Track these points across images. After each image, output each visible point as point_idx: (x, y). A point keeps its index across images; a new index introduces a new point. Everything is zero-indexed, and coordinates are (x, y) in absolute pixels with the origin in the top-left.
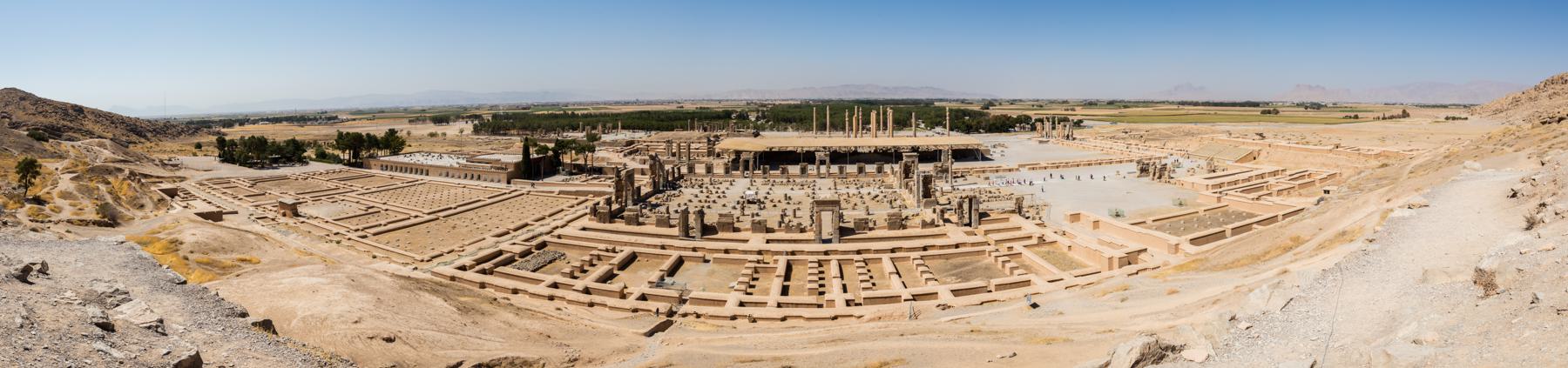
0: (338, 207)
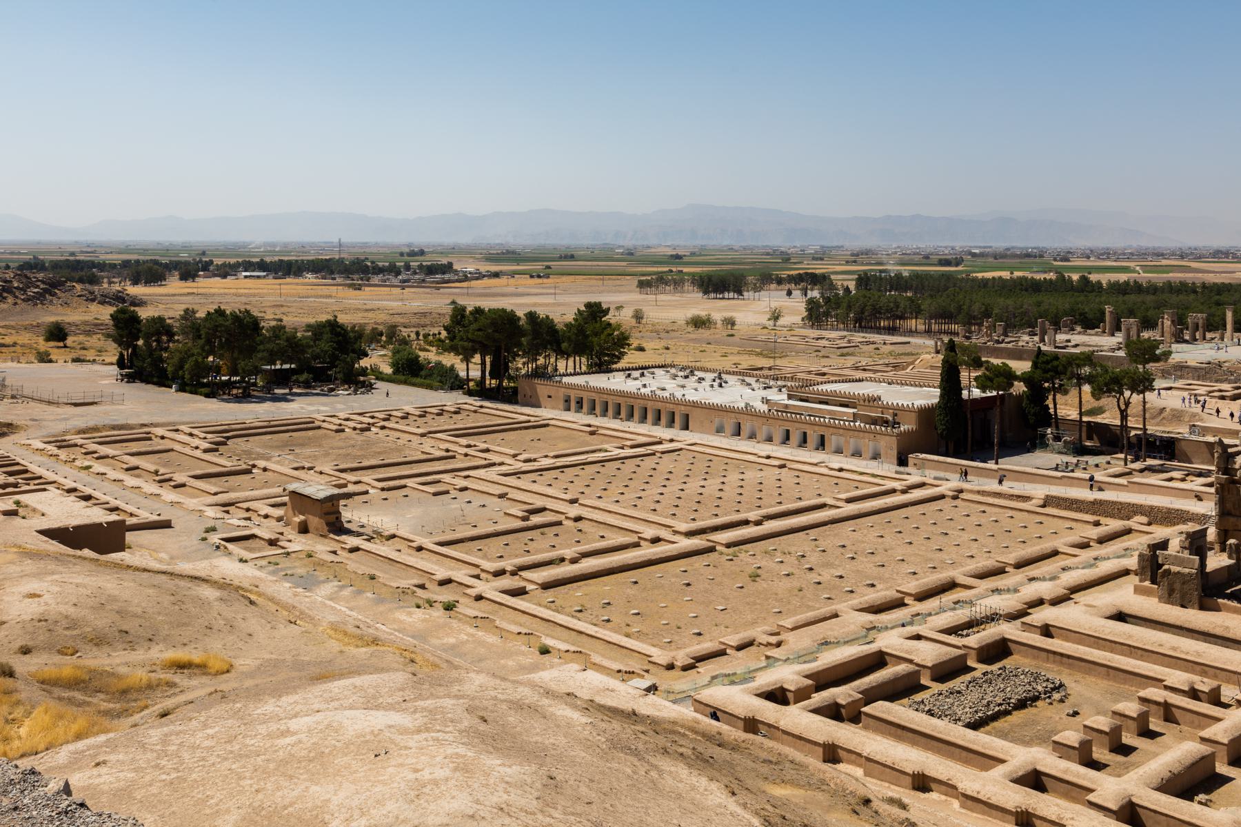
0: (452, 507)
